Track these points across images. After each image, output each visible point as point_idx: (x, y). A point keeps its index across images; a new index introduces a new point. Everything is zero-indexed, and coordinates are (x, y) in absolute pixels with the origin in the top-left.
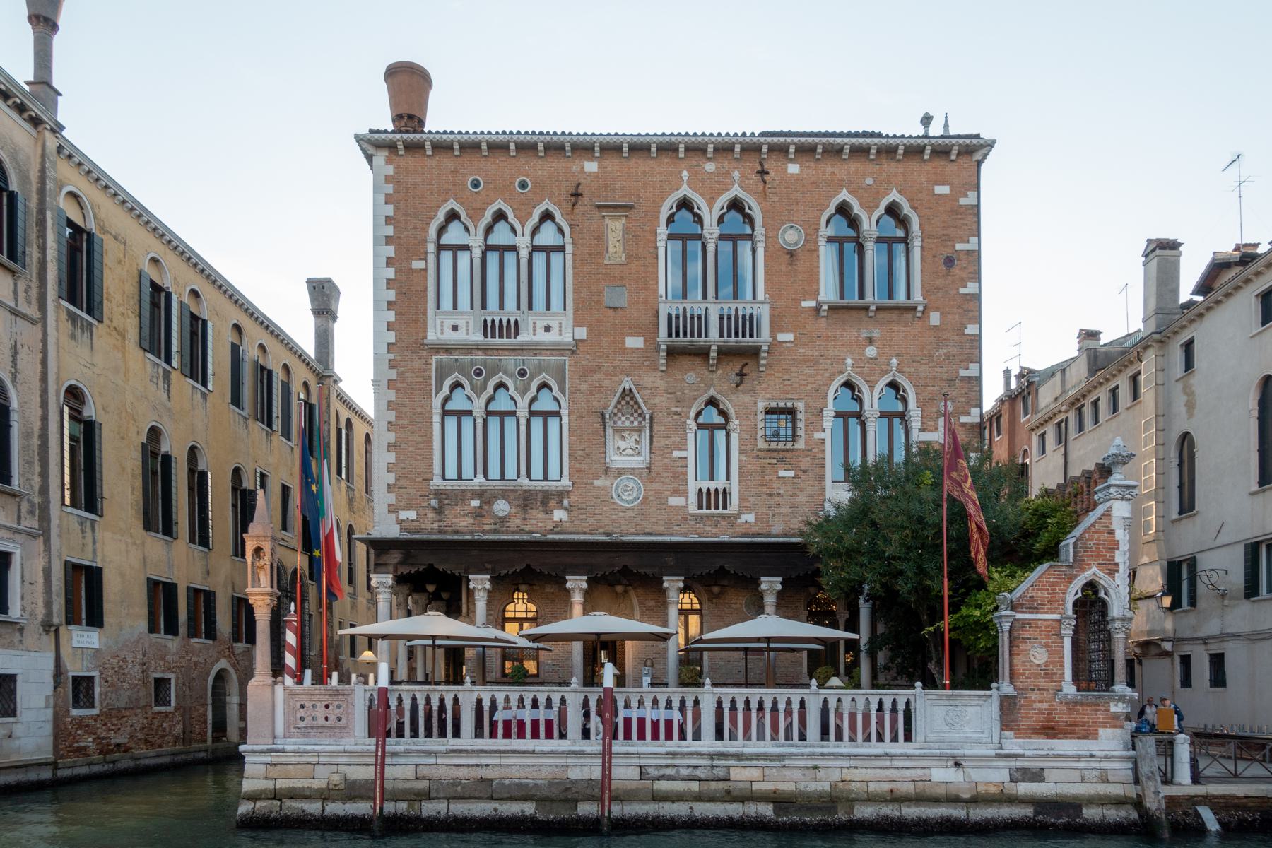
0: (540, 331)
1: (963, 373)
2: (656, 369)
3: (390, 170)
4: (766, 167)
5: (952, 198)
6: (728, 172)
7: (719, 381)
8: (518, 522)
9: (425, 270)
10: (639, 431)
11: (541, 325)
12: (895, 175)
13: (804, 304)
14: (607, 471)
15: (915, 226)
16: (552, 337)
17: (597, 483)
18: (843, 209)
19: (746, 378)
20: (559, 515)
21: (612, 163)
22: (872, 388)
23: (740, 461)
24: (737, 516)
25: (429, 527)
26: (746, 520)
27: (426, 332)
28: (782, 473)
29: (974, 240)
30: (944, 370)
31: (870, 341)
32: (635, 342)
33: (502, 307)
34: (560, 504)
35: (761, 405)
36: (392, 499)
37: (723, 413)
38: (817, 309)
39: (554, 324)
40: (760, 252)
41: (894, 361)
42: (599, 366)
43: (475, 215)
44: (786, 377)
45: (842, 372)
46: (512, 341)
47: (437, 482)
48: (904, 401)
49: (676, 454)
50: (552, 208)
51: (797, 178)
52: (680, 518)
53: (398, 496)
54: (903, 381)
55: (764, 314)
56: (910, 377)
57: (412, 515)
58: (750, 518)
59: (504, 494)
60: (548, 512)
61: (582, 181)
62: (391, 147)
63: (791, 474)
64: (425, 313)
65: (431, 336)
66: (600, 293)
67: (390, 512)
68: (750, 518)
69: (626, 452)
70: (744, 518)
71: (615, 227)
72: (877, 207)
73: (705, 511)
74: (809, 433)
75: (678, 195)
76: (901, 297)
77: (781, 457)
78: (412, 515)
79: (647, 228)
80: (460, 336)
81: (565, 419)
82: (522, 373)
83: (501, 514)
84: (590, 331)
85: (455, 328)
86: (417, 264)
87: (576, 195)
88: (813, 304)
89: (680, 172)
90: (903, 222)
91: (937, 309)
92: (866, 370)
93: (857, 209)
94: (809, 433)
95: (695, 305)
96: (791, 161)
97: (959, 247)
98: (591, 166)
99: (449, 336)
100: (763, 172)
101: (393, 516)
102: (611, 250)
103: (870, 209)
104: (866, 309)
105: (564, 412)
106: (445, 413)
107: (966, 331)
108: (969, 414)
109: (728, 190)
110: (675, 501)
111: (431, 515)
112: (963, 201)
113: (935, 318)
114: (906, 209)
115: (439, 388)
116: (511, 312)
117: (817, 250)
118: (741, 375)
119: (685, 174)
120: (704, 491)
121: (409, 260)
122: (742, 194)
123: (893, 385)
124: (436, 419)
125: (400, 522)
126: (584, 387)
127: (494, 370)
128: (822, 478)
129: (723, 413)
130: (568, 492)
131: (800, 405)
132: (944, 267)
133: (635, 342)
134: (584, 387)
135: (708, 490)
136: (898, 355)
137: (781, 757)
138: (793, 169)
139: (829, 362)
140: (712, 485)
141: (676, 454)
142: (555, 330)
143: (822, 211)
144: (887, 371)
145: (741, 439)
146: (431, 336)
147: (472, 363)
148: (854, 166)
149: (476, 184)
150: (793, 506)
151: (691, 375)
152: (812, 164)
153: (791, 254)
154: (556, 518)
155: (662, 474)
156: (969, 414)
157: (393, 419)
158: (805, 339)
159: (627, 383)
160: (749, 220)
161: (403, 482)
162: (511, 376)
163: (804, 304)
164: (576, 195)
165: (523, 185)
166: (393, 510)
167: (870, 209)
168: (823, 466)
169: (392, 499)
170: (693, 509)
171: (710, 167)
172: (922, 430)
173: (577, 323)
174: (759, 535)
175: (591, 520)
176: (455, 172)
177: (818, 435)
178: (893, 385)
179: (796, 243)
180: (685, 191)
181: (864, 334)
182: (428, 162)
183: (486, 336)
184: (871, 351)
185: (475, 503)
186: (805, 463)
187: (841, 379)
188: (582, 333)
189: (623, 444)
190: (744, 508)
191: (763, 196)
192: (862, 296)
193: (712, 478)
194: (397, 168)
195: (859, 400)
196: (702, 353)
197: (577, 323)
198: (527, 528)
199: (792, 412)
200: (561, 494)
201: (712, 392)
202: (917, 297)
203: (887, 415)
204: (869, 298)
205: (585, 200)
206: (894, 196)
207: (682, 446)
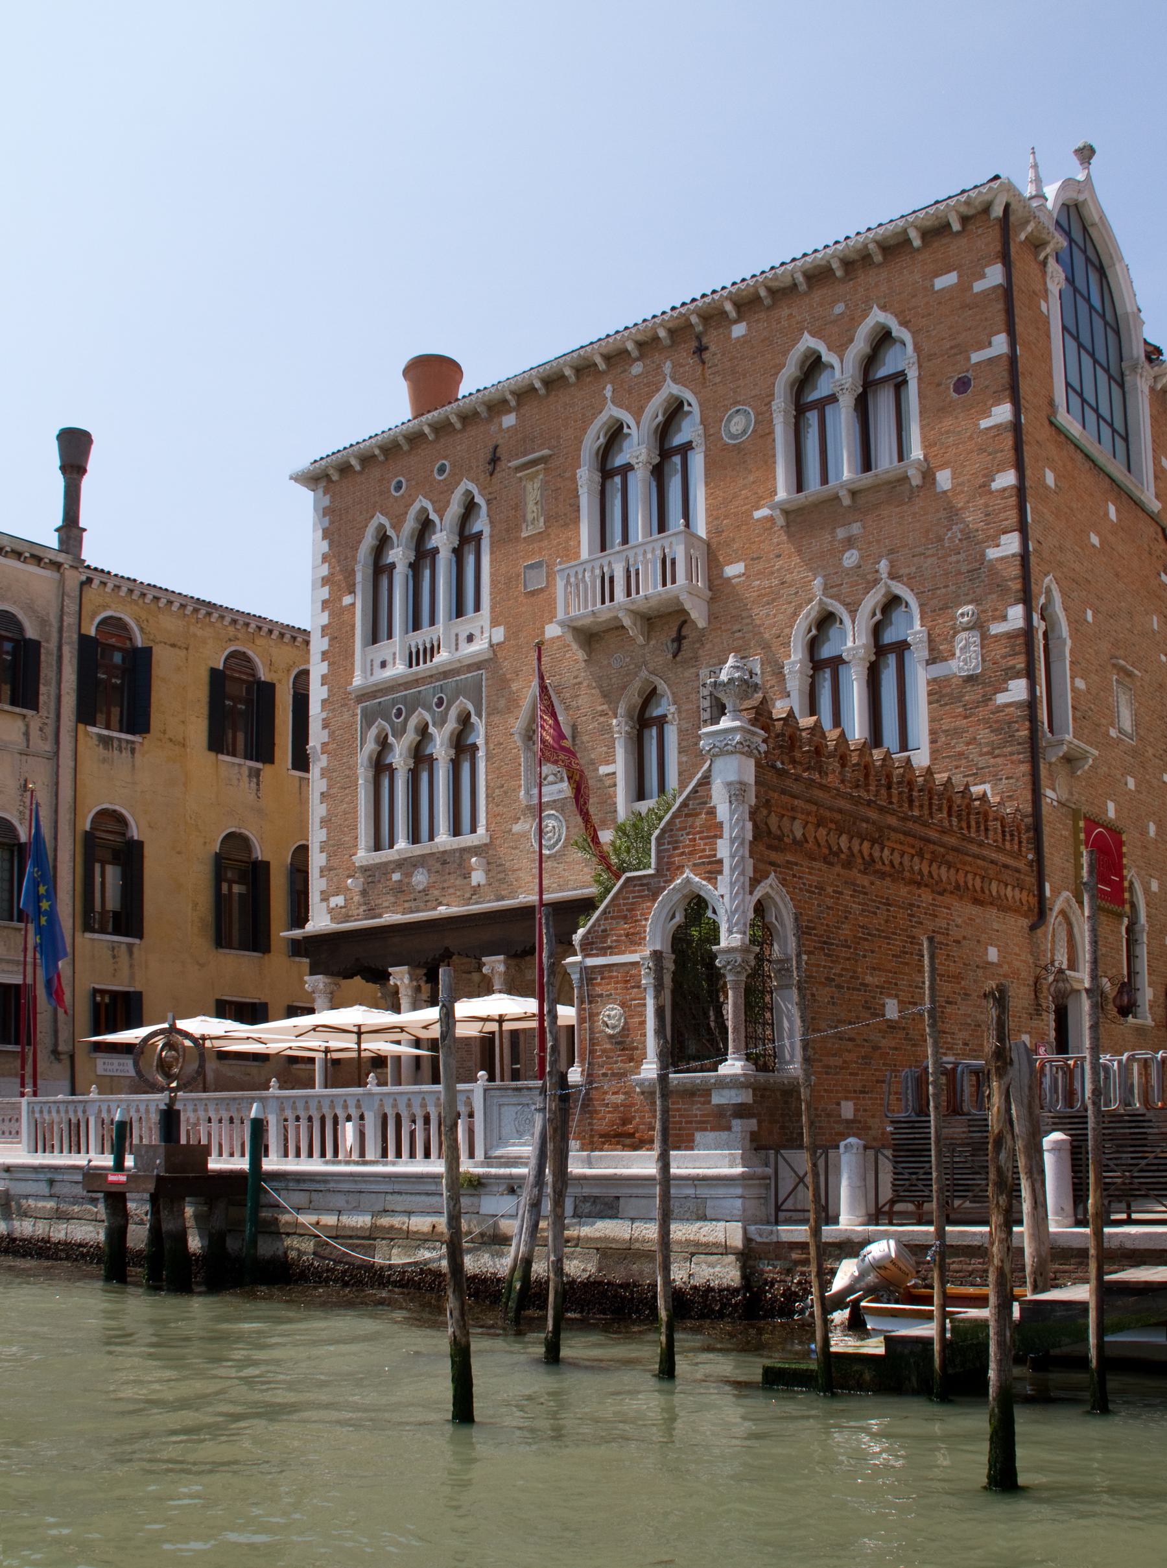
4: (705, 340)
5: (964, 286)
6: (659, 367)
12: (877, 285)
17: (517, 828)
19: (685, 642)
22: (853, 613)
23: (680, 763)
30: (962, 557)
31: (850, 543)
41: (883, 566)
44: (736, 628)
45: (811, 600)
47: (363, 855)
51: (744, 341)
60: (467, 876)
61: (500, 441)
72: (851, 340)
75: (603, 418)
79: (567, 475)
83: (421, 887)
89: (604, 388)
91: (943, 466)
92: (845, 589)
96: (736, 322)
97: (976, 357)
100: (701, 350)
102: (530, 517)
103: (839, 349)
107: (995, 486)
108: (1004, 618)
109: (658, 390)
113: (944, 479)
117: (772, 432)
119: (609, 387)
127: (413, 705)
130: (486, 845)
132: (955, 396)
136: (892, 552)
138: (739, 330)
139: (793, 590)
144: (876, 581)
145: (680, 731)
148: (817, 295)
152: (763, 315)
153: (738, 448)
154: (474, 883)
156: (1004, 618)
158: (760, 566)
164: (494, 460)
167: (839, 349)
173: (494, 623)
179: (744, 432)
181: (841, 533)
184: (850, 558)
185: (396, 877)
191: (699, 384)
205: (503, 464)
207: (609, 759)
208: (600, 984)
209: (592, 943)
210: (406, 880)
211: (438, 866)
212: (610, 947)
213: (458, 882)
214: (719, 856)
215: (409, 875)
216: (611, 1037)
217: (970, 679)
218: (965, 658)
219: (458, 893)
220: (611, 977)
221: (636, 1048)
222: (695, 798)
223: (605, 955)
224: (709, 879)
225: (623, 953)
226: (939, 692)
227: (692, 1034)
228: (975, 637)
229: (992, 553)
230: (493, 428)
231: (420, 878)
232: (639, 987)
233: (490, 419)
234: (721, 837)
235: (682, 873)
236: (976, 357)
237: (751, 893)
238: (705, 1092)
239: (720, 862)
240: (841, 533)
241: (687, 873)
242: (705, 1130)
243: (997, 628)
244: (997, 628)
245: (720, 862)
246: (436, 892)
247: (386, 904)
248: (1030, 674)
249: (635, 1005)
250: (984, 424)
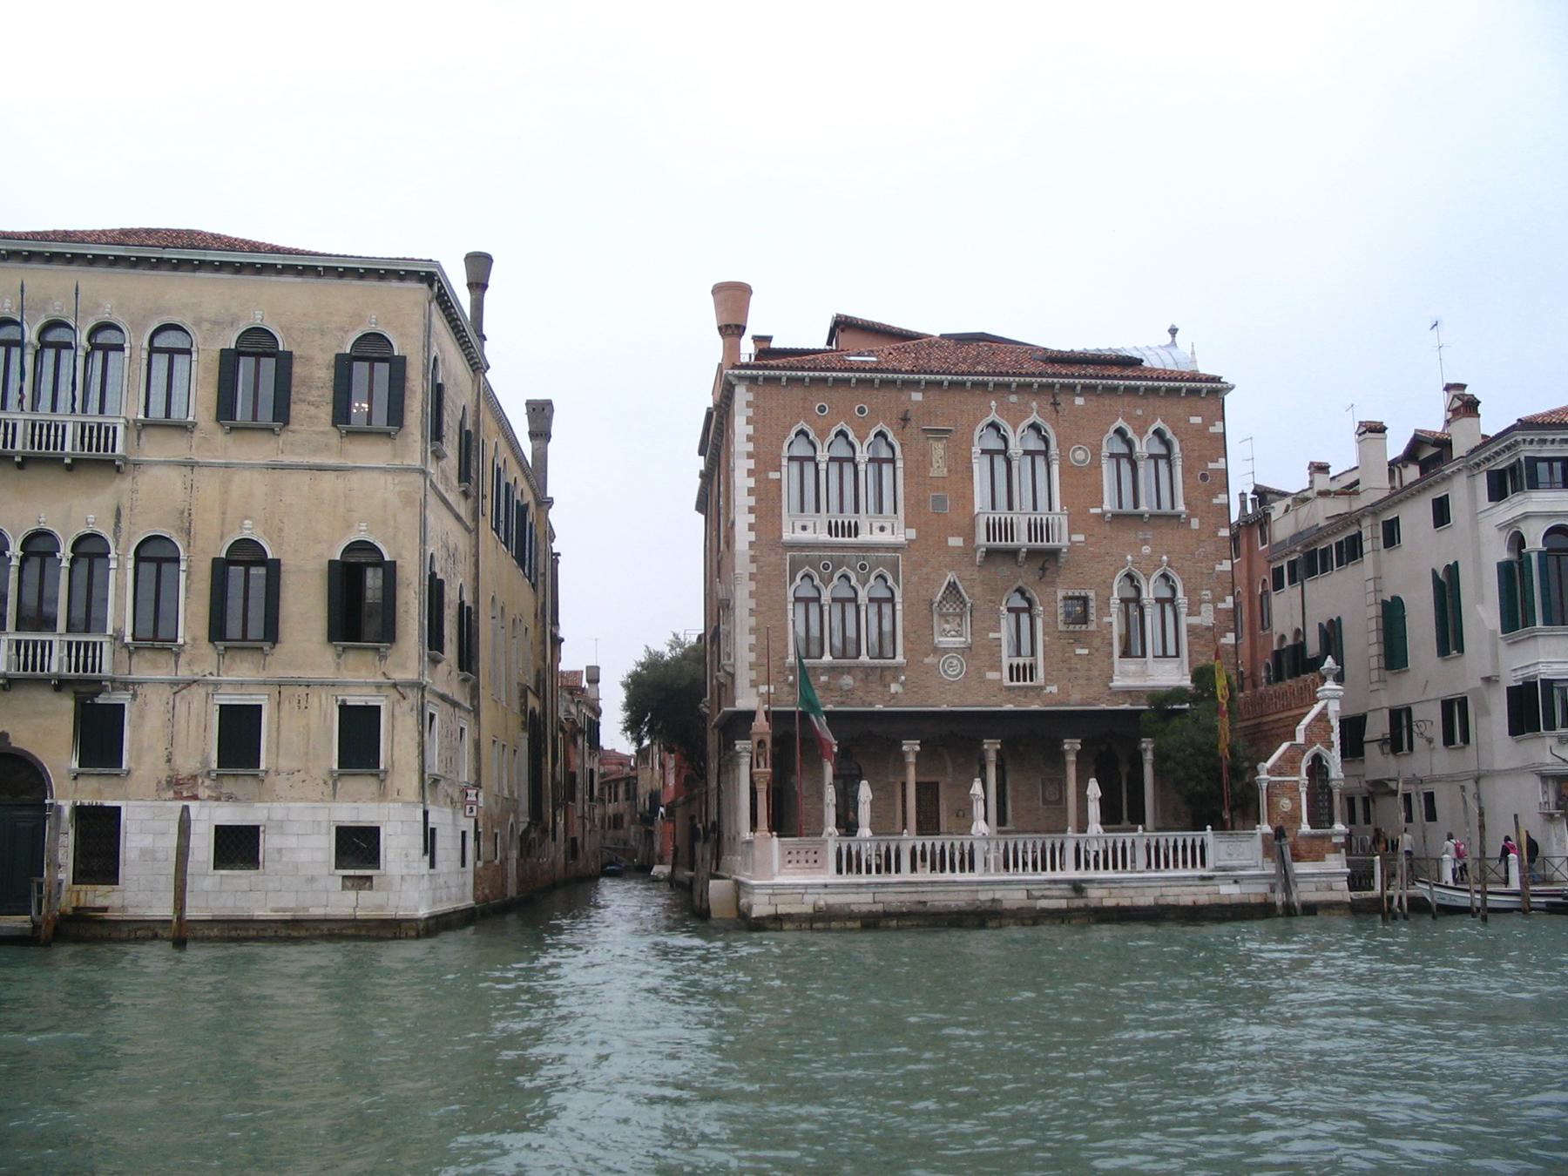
0: (876, 530)
1: (1218, 568)
2: (973, 564)
3: (750, 397)
7: (1026, 576)
9: (780, 480)
10: (961, 616)
11: (876, 526)
13: (1093, 511)
14: (936, 650)
15: (1176, 449)
16: (885, 538)
17: (927, 660)
18: (1120, 432)
20: (894, 688)
21: (934, 394)
24: (1042, 688)
26: (1052, 691)
27: (780, 530)
28: (1078, 651)
29: (1222, 460)
31: (1145, 542)
32: (955, 541)
33: (842, 511)
34: (896, 679)
35: (1061, 594)
36: (753, 675)
37: (1029, 601)
38: (1103, 515)
39: (888, 525)
40: (1055, 469)
42: (927, 561)
43: (822, 435)
46: (853, 539)
48: (1174, 590)
49: (992, 635)
50: (886, 429)
52: (995, 691)
54: (1171, 573)
55: (1059, 518)
56: (1177, 570)
58: (1054, 689)
59: (849, 670)
62: (753, 380)
63: (1086, 651)
64: (780, 516)
65: (787, 536)
66: (926, 501)
68: (1054, 689)
69: (949, 638)
70: (1049, 689)
71: (938, 449)
73: (1015, 683)
74: (1099, 617)
75: (989, 420)
76: (1166, 507)
77: (1078, 639)
80: (808, 536)
81: (899, 607)
82: (863, 567)
84: (918, 533)
85: (804, 528)
86: (773, 475)
87: (905, 419)
88: (1098, 511)
90: (1167, 444)
93: (1130, 434)
94: (1099, 617)
95: (1002, 514)
97: (1211, 466)
98: (917, 396)
99: (801, 536)
100: (1055, 404)
104: (1141, 516)
105: (898, 599)
106: (797, 600)
110: (992, 675)
111: (786, 689)
112: (1212, 429)
113: (1195, 523)
114: (1169, 435)
115: (792, 580)
116: (849, 517)
118: (1043, 569)
121: (766, 472)
122: (1039, 421)
123: (1165, 576)
124: (790, 606)
125: (760, 695)
126: (915, 579)
127: (837, 567)
128: (1111, 655)
129: (1029, 601)
131: (1092, 594)
133: (955, 541)
134: (915, 579)
136: (1167, 553)
138: (1079, 401)
140: (1021, 661)
141: (992, 635)
142: (889, 530)
143: (1103, 435)
146: (787, 536)
147: (821, 558)
148: (1126, 400)
149: (822, 409)
150: (1088, 679)
151: (1004, 570)
155: (980, 653)
157: (753, 606)
159: (951, 577)
160: (1046, 441)
162: (853, 569)
163: (1093, 511)
165: (861, 411)
166: (754, 684)
168: (1111, 645)
169: (753, 675)
170: (1007, 682)
171: (1013, 398)
172: (1189, 615)
174: (1062, 704)
176: (804, 399)
177: (1106, 619)
178: (1165, 576)
180: (993, 417)
182: (782, 391)
183: (830, 533)
184: (1146, 550)
186: (1097, 642)
187: (1123, 572)
188: (912, 534)
189: (947, 627)
190: (1049, 680)
191: (1055, 425)
192: (1136, 505)
193: (1019, 654)
194: (757, 396)
195: (1138, 590)
196: (1014, 553)
197: (907, 526)
198: (869, 699)
199: (1085, 600)
200: (897, 669)
201: (1020, 583)
202: (1181, 507)
203: (1161, 601)
204: (1143, 508)
205: (913, 424)
206: (1159, 424)
207: (997, 629)
217: (1208, 628)
218: (1206, 617)
226: (1192, 630)
228: (1211, 607)
229: (1218, 568)
230: (904, 397)
231: (847, 681)
233: (900, 390)
236: (1211, 466)
238: (1329, 837)
240: (1141, 535)
243: (1221, 606)
244: (1221, 606)
248: (1235, 631)
250: (1215, 501)
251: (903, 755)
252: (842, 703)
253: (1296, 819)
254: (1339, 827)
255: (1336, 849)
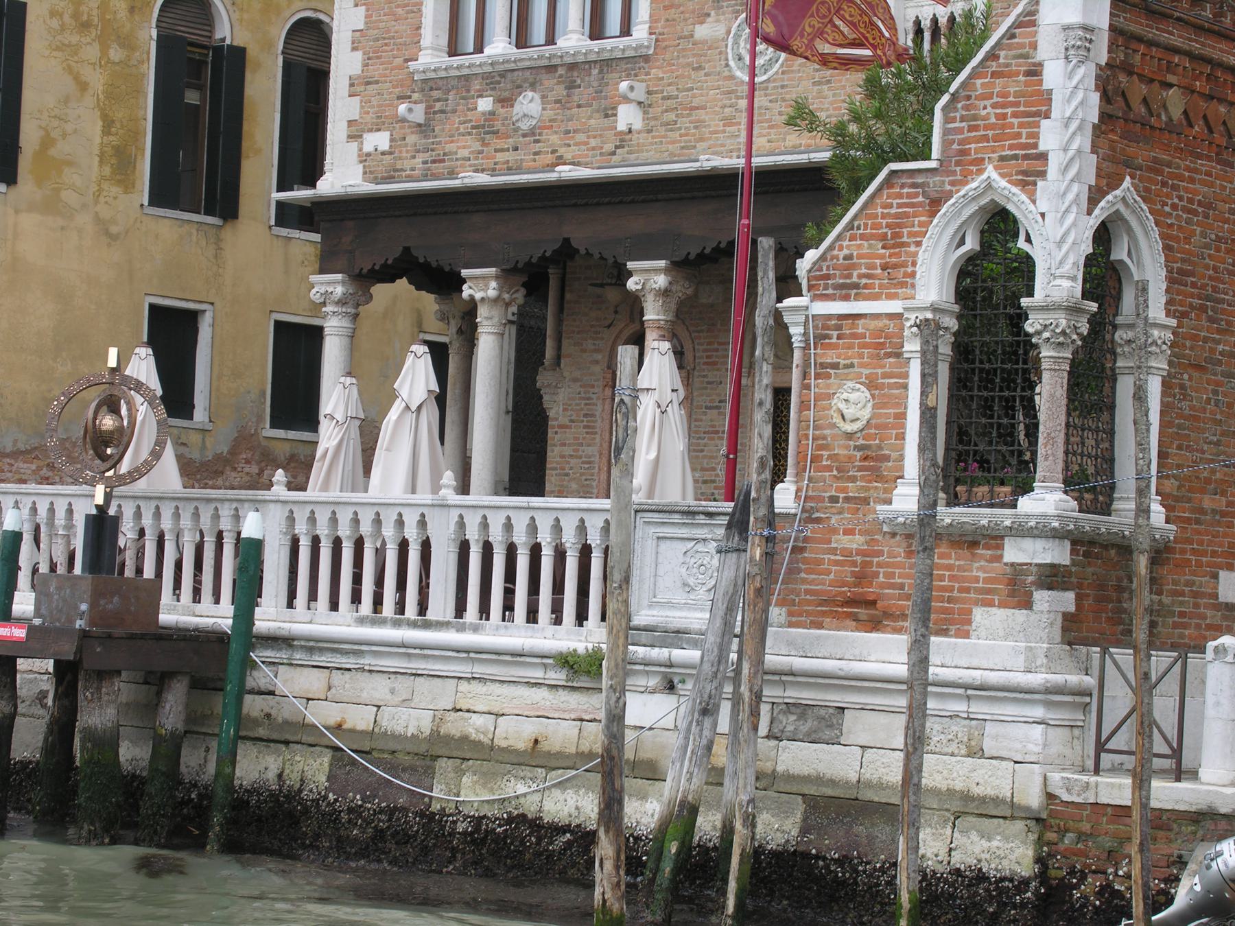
8: (555, 139)
17: (702, 32)
25: (407, 164)
53: (365, 103)
57: (379, 141)
60: (610, 113)
67: (351, 137)
78: (379, 141)
83: (525, 126)
101: (354, 145)
120: (926, 24)
125: (364, 158)
130: (646, 58)
135: (935, 21)
137: (355, 647)
154: (621, 126)
161: (376, 70)
175: (684, 122)
208: (835, 346)
209: (827, 277)
210: (502, 111)
211: (560, 91)
212: (856, 286)
213: (592, 122)
214: (1042, 147)
215: (506, 101)
216: (850, 436)
219: (593, 143)
220: (854, 336)
221: (887, 458)
222: (1010, 47)
223: (846, 298)
224: (1023, 185)
225: (876, 297)
227: (984, 435)
231: (529, 105)
232: (898, 355)
234: (1047, 117)
235: (980, 172)
237: (1089, 213)
238: (993, 539)
239: (1043, 157)
241: (991, 172)
242: (990, 604)
245: (1043, 157)
246: (555, 139)
247: (464, 153)
249: (891, 386)
251: (634, 304)
252: (519, 170)
253: (876, 464)
254: (1046, 500)
255: (1017, 589)
